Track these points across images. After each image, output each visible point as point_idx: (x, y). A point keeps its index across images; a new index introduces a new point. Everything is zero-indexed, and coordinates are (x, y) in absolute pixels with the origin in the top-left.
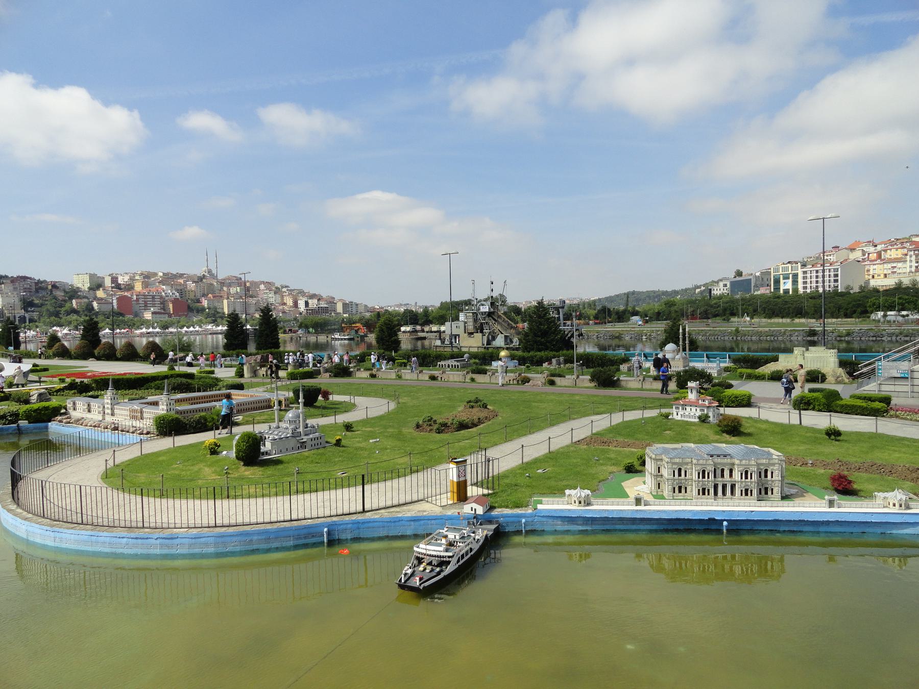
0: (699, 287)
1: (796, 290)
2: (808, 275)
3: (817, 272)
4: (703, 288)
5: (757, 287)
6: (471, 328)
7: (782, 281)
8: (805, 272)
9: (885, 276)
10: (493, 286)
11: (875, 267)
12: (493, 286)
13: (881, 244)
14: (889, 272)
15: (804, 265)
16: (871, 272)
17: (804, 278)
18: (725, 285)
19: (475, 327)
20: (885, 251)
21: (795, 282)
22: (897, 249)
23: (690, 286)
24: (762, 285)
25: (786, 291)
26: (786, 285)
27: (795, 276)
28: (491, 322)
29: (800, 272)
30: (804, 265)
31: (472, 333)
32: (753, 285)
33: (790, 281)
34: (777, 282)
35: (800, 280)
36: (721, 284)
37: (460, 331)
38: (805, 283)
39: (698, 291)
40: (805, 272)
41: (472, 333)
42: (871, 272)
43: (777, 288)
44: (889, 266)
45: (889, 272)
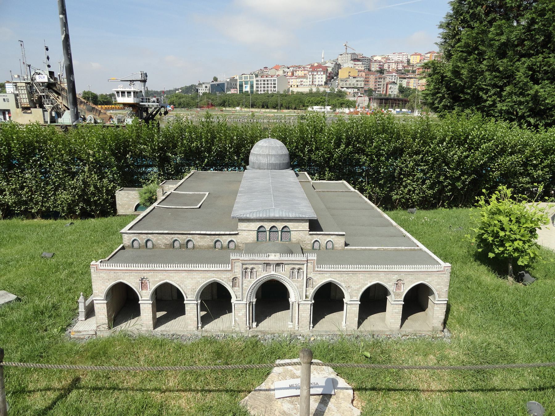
0: (178, 90)
1: (252, 92)
2: (259, 83)
3: (264, 81)
4: (180, 91)
5: (228, 89)
6: (25, 100)
7: (244, 86)
8: (257, 81)
9: (297, 86)
10: (49, 53)
11: (292, 80)
12: (49, 53)
13: (292, 67)
14: (299, 84)
15: (257, 76)
16: (290, 84)
17: (257, 84)
18: (206, 87)
19: (31, 101)
20: (296, 71)
21: (252, 87)
22: (302, 71)
23: (172, 89)
24: (231, 88)
26: (247, 88)
28: (53, 96)
29: (254, 80)
30: (257, 76)
31: (28, 108)
32: (226, 87)
33: (249, 86)
34: (241, 86)
35: (255, 86)
36: (204, 86)
37: (11, 105)
38: (257, 87)
39: (177, 92)
40: (257, 81)
41: (28, 108)
42: (290, 84)
43: (241, 90)
44: (299, 80)
45: (299, 84)
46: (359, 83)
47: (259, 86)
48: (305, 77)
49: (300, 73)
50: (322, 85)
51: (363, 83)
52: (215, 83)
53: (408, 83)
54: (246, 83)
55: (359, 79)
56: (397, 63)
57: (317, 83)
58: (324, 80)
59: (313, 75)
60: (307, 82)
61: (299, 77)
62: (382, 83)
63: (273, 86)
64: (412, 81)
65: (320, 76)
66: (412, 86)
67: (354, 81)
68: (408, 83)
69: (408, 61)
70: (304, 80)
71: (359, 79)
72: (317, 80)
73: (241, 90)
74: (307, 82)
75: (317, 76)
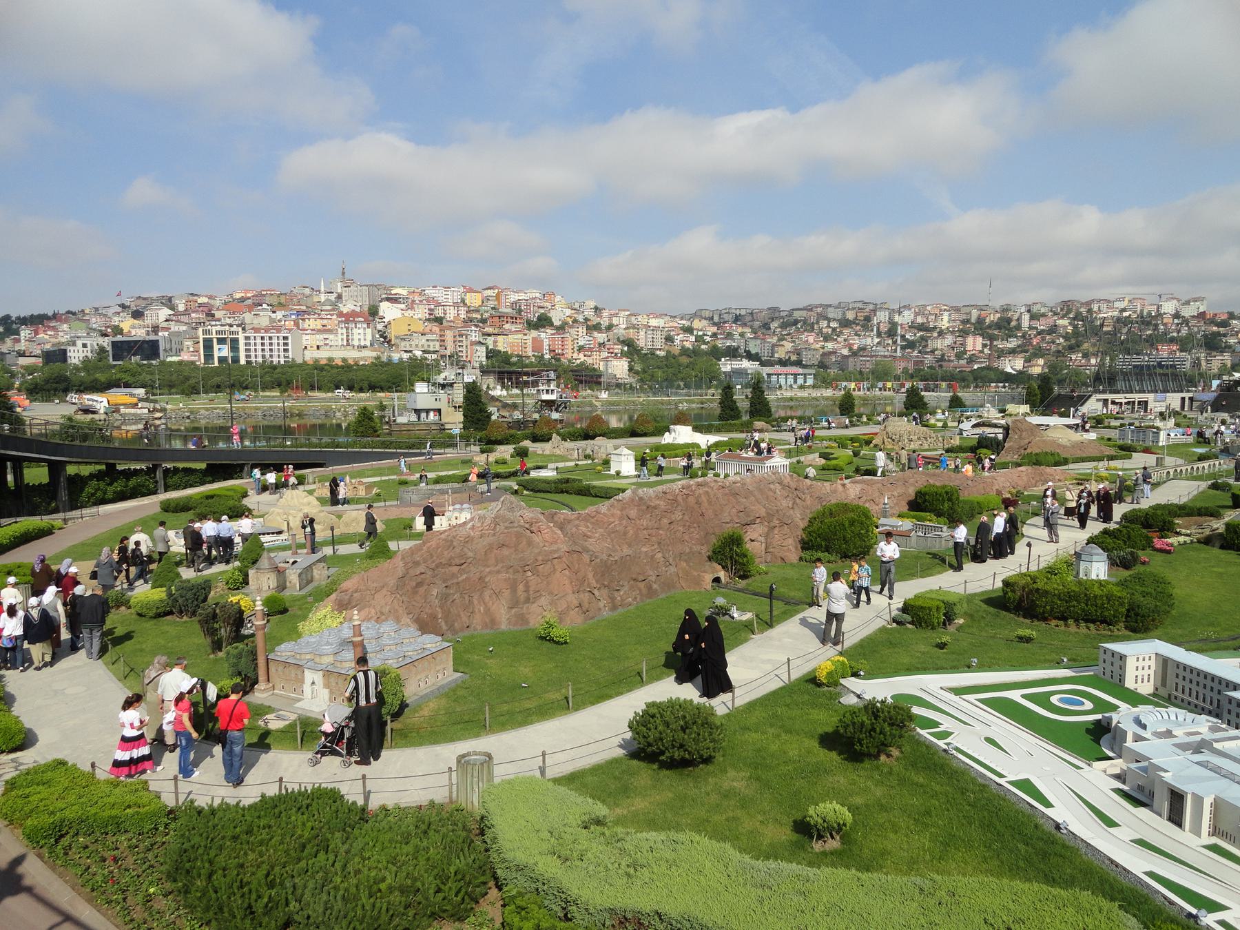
1: (236, 360)
2: (252, 342)
3: (263, 338)
7: (216, 347)
17: (246, 344)
18: (85, 346)
25: (221, 360)
27: (235, 342)
34: (208, 345)
35: (242, 347)
38: (248, 350)
40: (247, 338)
42: (305, 343)
43: (209, 356)
44: (321, 336)
45: (321, 343)
46: (431, 344)
47: (252, 348)
48: (324, 330)
49: (311, 323)
50: (365, 347)
51: (437, 344)
52: (119, 338)
53: (495, 342)
54: (221, 341)
55: (429, 337)
56: (456, 305)
57: (356, 343)
58: (369, 337)
59: (347, 328)
60: (338, 339)
61: (319, 332)
62: (464, 344)
63: (282, 348)
64: (500, 339)
65: (361, 331)
66: (501, 347)
67: (423, 340)
68: (495, 342)
69: (463, 301)
70: (331, 337)
71: (429, 337)
72: (356, 337)
73: (209, 356)
74: (338, 339)
75: (356, 331)
